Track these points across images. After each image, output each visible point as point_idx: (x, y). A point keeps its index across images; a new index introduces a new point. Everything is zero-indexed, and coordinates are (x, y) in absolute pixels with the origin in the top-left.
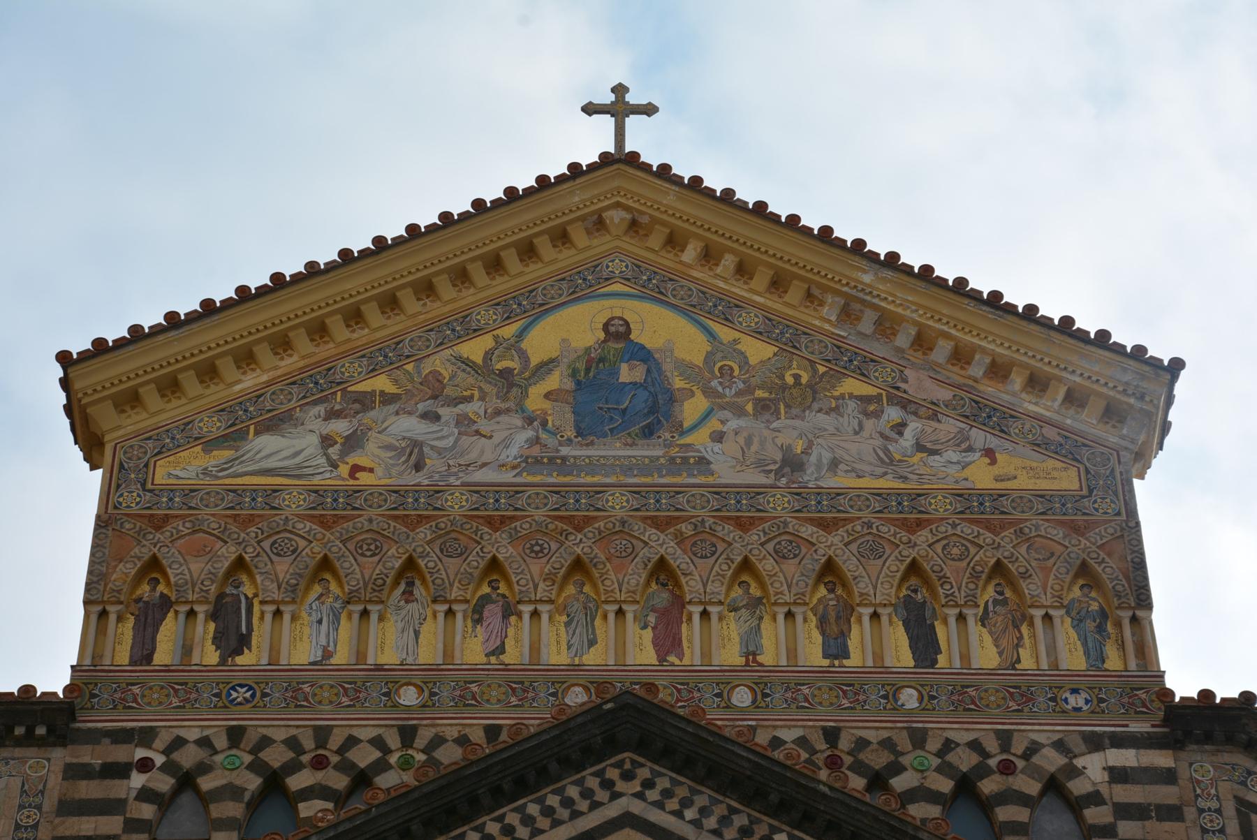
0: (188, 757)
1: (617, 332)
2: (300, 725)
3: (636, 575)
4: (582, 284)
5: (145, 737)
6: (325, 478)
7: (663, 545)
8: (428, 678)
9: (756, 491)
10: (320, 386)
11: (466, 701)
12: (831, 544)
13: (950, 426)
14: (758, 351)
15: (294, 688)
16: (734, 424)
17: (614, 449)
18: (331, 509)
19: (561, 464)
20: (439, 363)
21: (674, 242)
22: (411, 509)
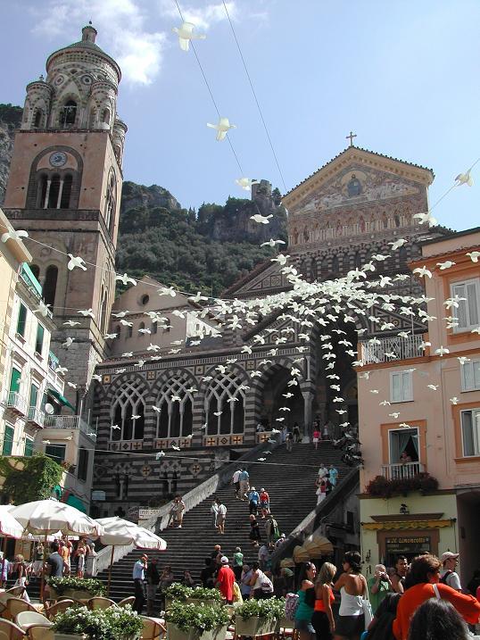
0: (303, 257)
1: (354, 177)
2: (316, 251)
3: (358, 220)
4: (348, 169)
5: (297, 255)
6: (316, 210)
7: (361, 213)
8: (332, 241)
9: (373, 202)
10: (314, 195)
11: (336, 244)
12: (384, 209)
13: (401, 185)
14: (374, 176)
15: (314, 246)
16: (371, 190)
17: (354, 198)
18: (317, 215)
19: (346, 202)
20: (329, 187)
21: (361, 159)
22: (328, 213)
